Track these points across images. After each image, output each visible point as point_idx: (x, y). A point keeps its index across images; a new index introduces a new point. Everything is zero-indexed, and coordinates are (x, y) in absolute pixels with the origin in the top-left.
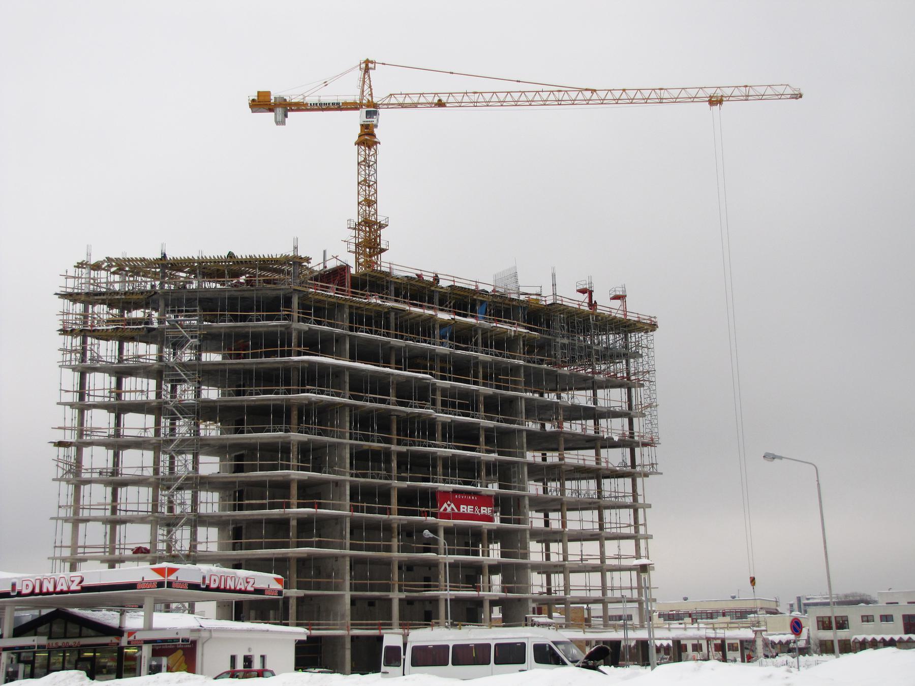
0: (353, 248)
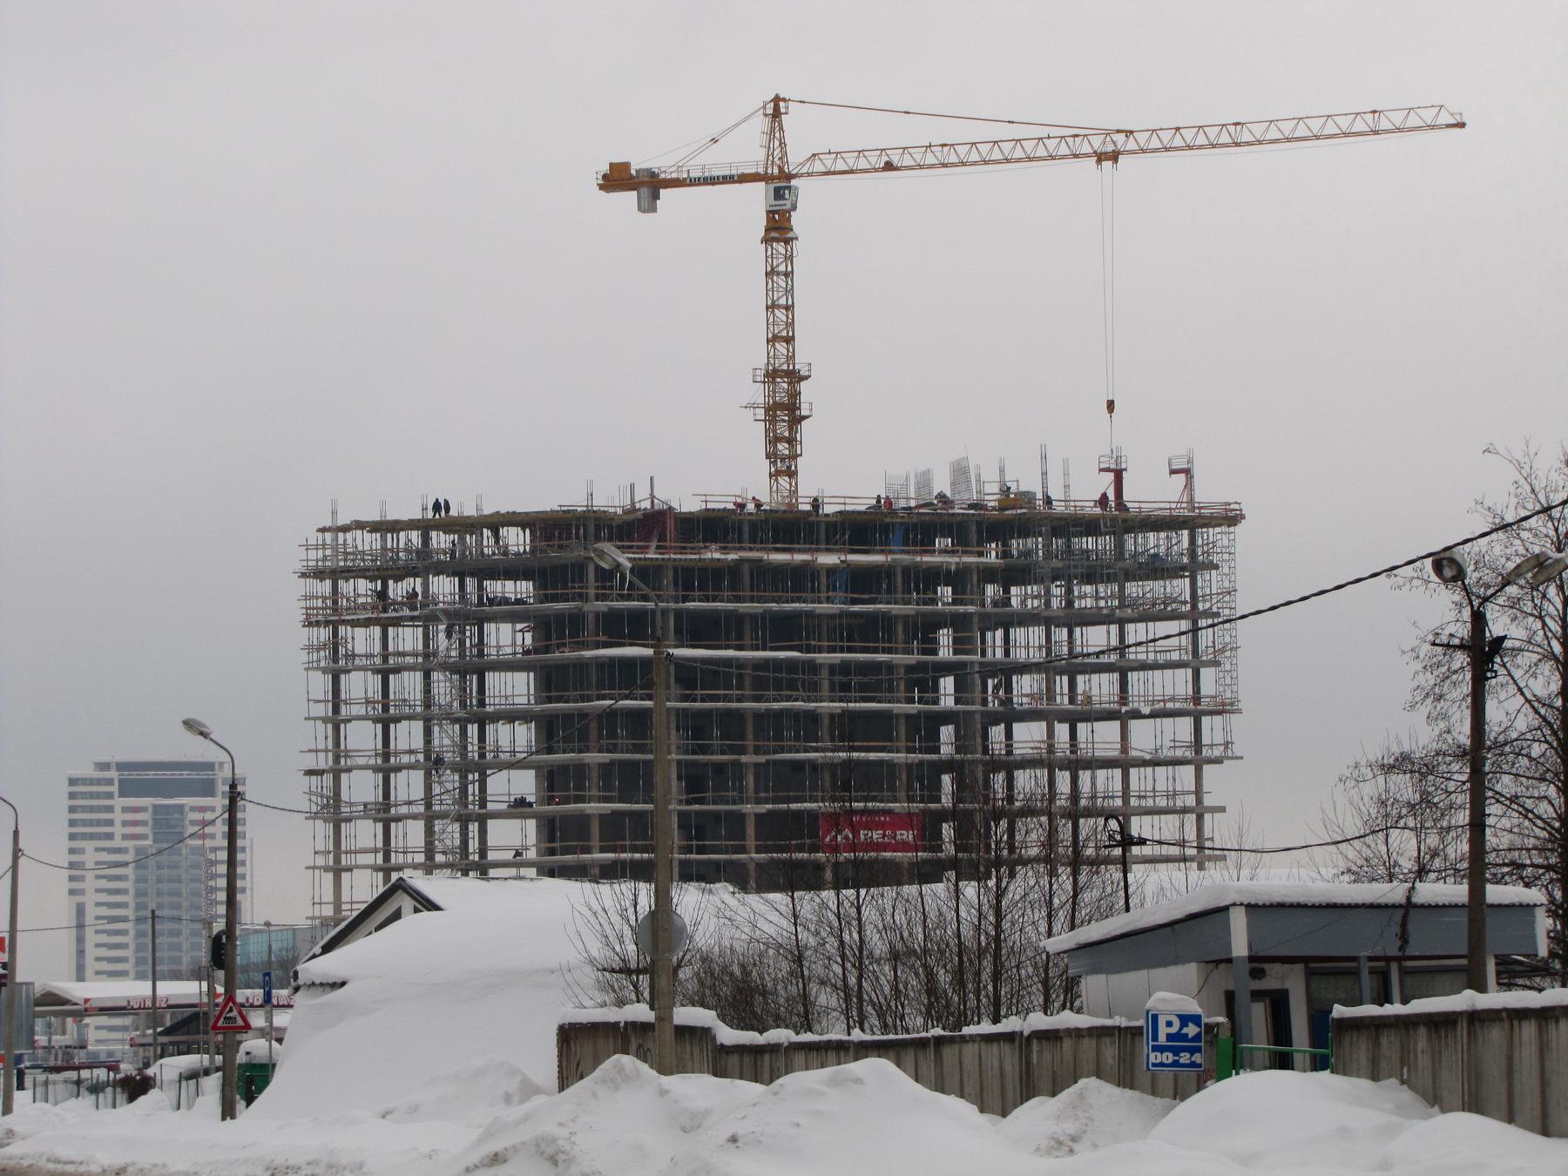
0: (761, 413)
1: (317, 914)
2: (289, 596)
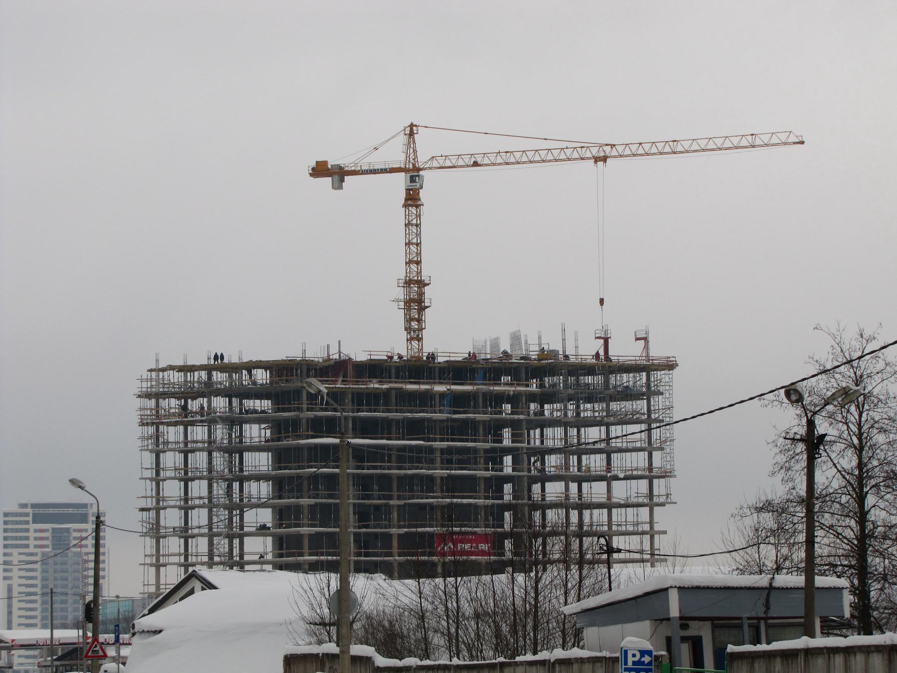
0: (402, 304)
1: (146, 591)
2: (132, 408)
